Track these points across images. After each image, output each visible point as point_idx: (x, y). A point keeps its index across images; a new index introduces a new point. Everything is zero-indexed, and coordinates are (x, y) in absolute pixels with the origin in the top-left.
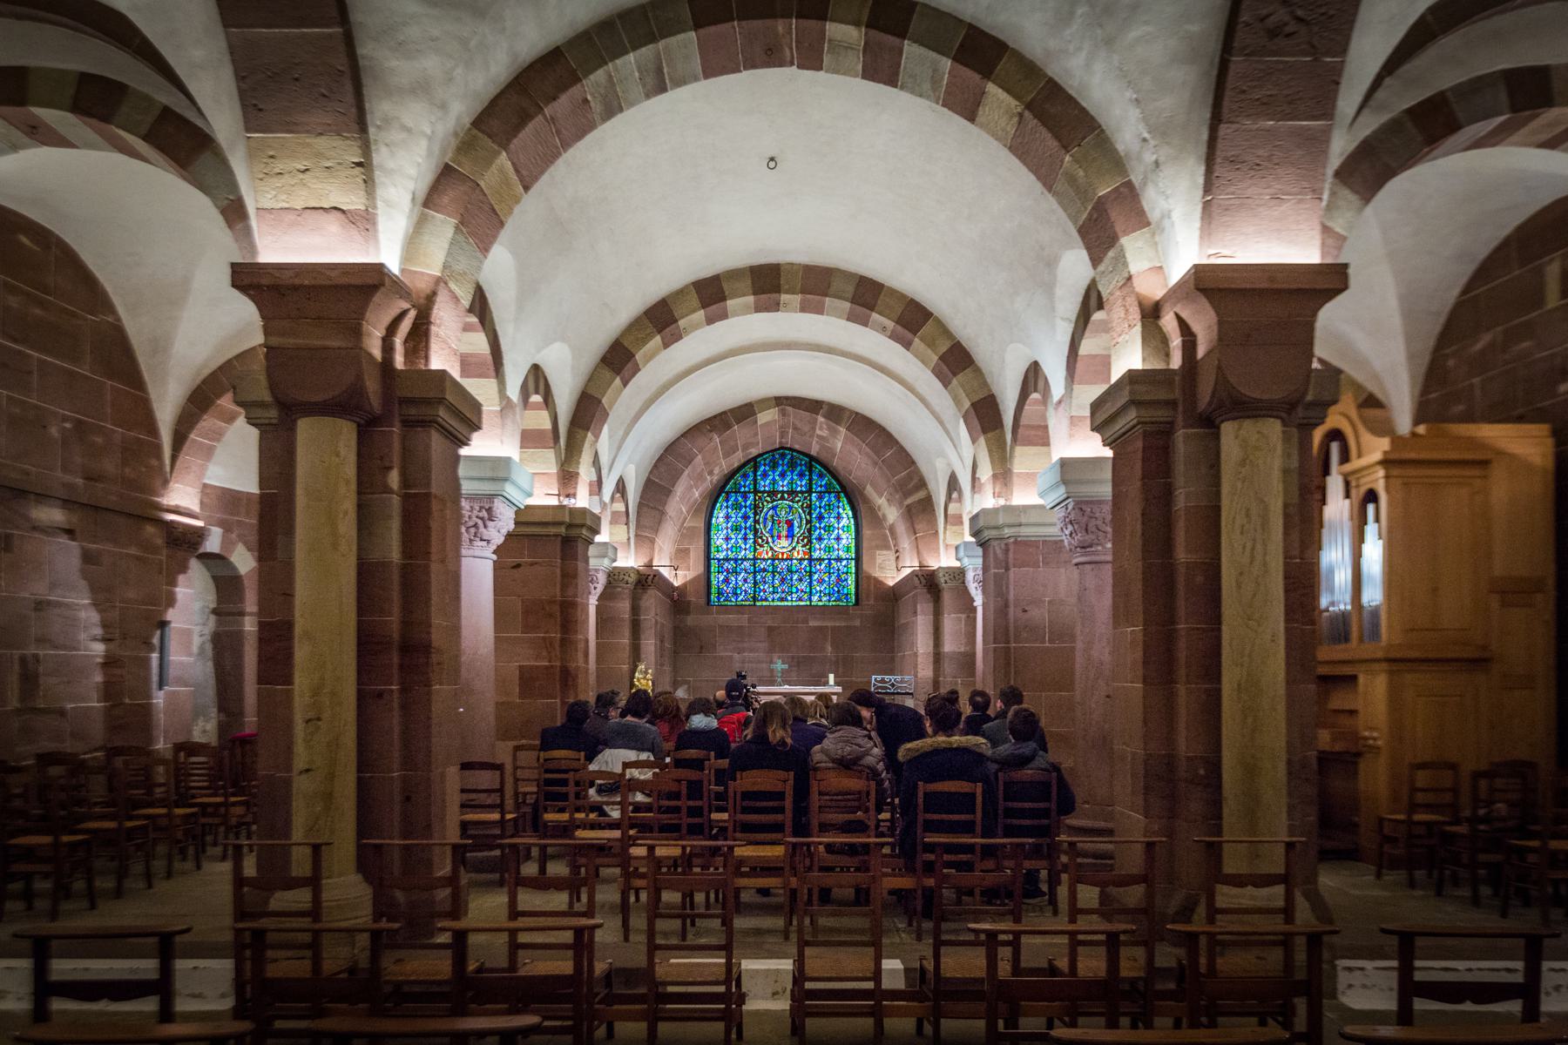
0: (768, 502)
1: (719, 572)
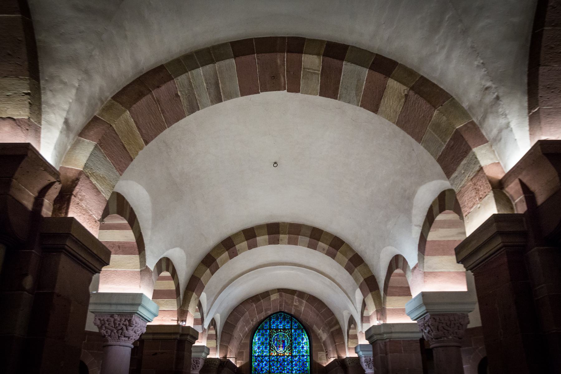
1: (255, 361)
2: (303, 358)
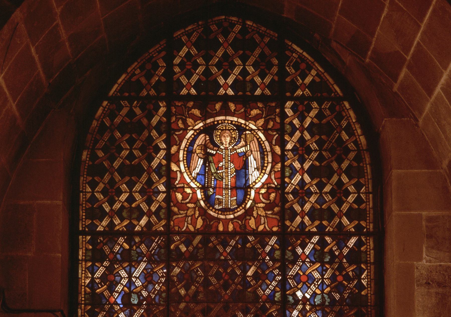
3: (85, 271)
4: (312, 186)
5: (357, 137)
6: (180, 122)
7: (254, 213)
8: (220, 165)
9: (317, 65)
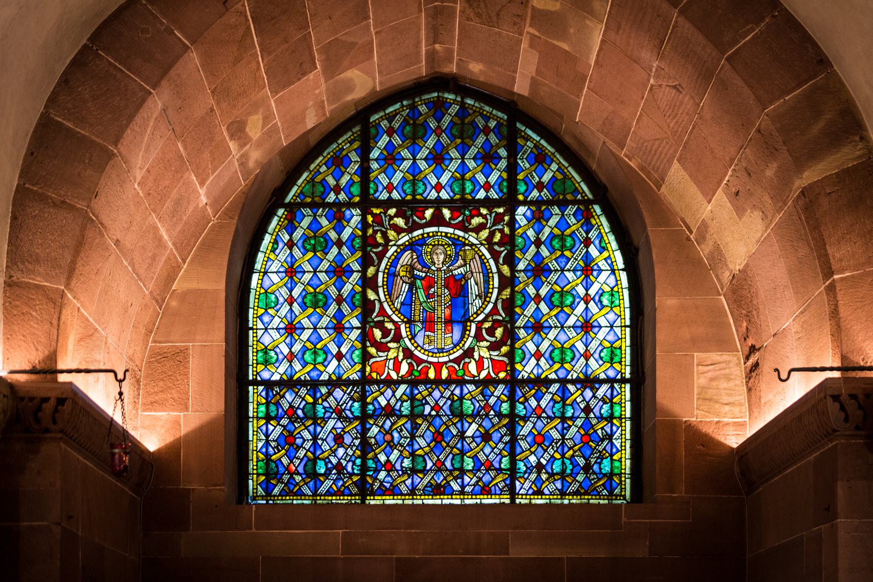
0: (398, 230)
1: (268, 418)
2: (588, 394)
3: (257, 431)
4: (551, 318)
5: (611, 252)
6: (379, 235)
7: (475, 354)
8: (431, 292)
9: (558, 156)
